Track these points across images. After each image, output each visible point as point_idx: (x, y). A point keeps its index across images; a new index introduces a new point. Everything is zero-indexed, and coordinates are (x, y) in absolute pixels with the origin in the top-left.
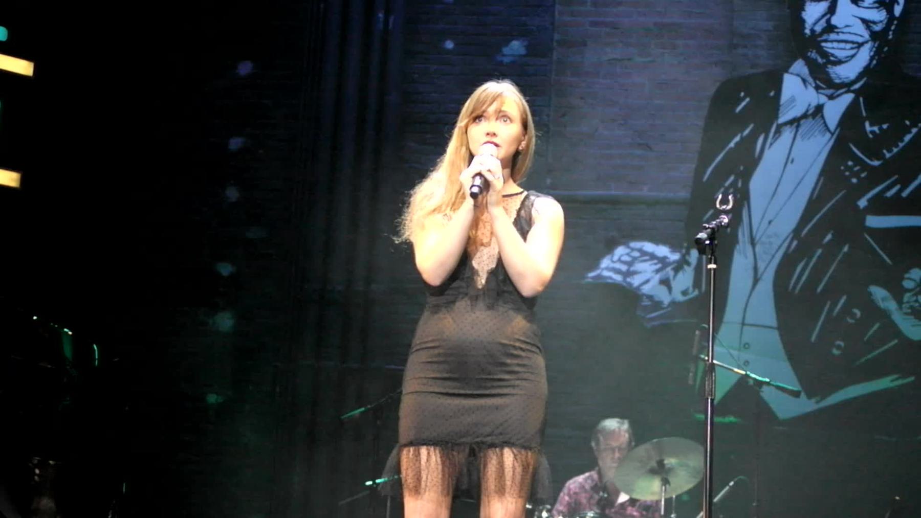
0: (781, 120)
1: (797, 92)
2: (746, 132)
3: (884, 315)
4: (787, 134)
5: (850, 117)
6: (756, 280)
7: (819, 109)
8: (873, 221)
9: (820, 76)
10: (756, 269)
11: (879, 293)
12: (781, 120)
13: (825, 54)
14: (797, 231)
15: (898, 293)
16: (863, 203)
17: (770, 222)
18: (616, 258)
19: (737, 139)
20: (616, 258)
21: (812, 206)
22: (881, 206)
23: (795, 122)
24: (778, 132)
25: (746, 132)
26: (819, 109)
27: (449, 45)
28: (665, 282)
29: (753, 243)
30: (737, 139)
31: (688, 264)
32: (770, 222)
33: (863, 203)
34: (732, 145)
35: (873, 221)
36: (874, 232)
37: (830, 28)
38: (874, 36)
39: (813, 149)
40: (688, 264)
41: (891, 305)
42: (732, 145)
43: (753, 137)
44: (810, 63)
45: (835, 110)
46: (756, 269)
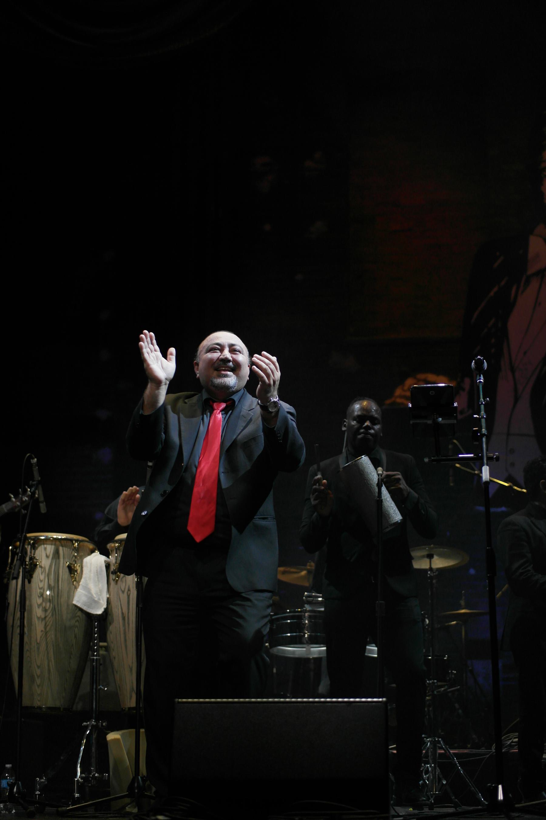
0: (530, 271)
2: (503, 283)
4: (534, 284)
6: (516, 399)
10: (516, 390)
12: (530, 271)
17: (525, 353)
18: (406, 388)
19: (496, 289)
20: (406, 388)
24: (528, 282)
25: (503, 283)
27: (267, 227)
29: (513, 370)
30: (496, 289)
31: (464, 390)
32: (525, 353)
34: (492, 294)
40: (464, 390)
42: (492, 294)
46: (516, 390)
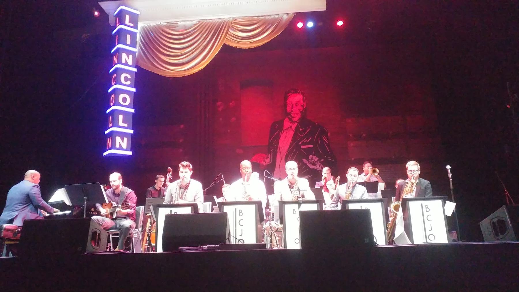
1: (287, 124)
3: (306, 164)
4: (285, 132)
5: (297, 127)
7: (291, 127)
8: (303, 147)
9: (291, 120)
11: (305, 160)
13: (291, 116)
14: (288, 150)
15: (308, 160)
16: (300, 143)
21: (291, 145)
22: (304, 144)
23: (287, 129)
26: (291, 127)
28: (264, 161)
33: (300, 143)
35: (303, 147)
36: (302, 149)
37: (292, 111)
38: (301, 112)
39: (291, 133)
41: (307, 162)
43: (279, 132)
44: (289, 119)
45: (294, 127)
